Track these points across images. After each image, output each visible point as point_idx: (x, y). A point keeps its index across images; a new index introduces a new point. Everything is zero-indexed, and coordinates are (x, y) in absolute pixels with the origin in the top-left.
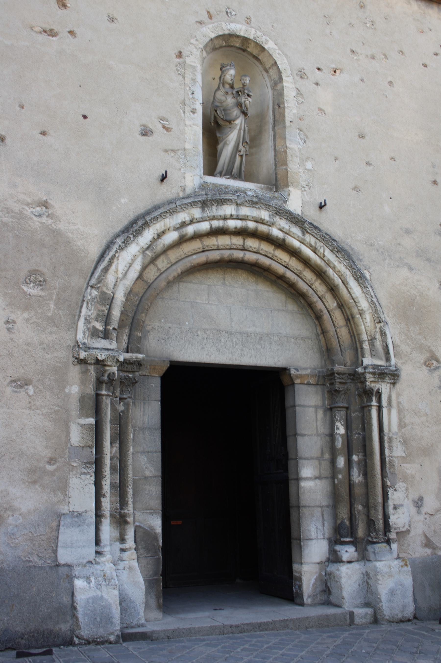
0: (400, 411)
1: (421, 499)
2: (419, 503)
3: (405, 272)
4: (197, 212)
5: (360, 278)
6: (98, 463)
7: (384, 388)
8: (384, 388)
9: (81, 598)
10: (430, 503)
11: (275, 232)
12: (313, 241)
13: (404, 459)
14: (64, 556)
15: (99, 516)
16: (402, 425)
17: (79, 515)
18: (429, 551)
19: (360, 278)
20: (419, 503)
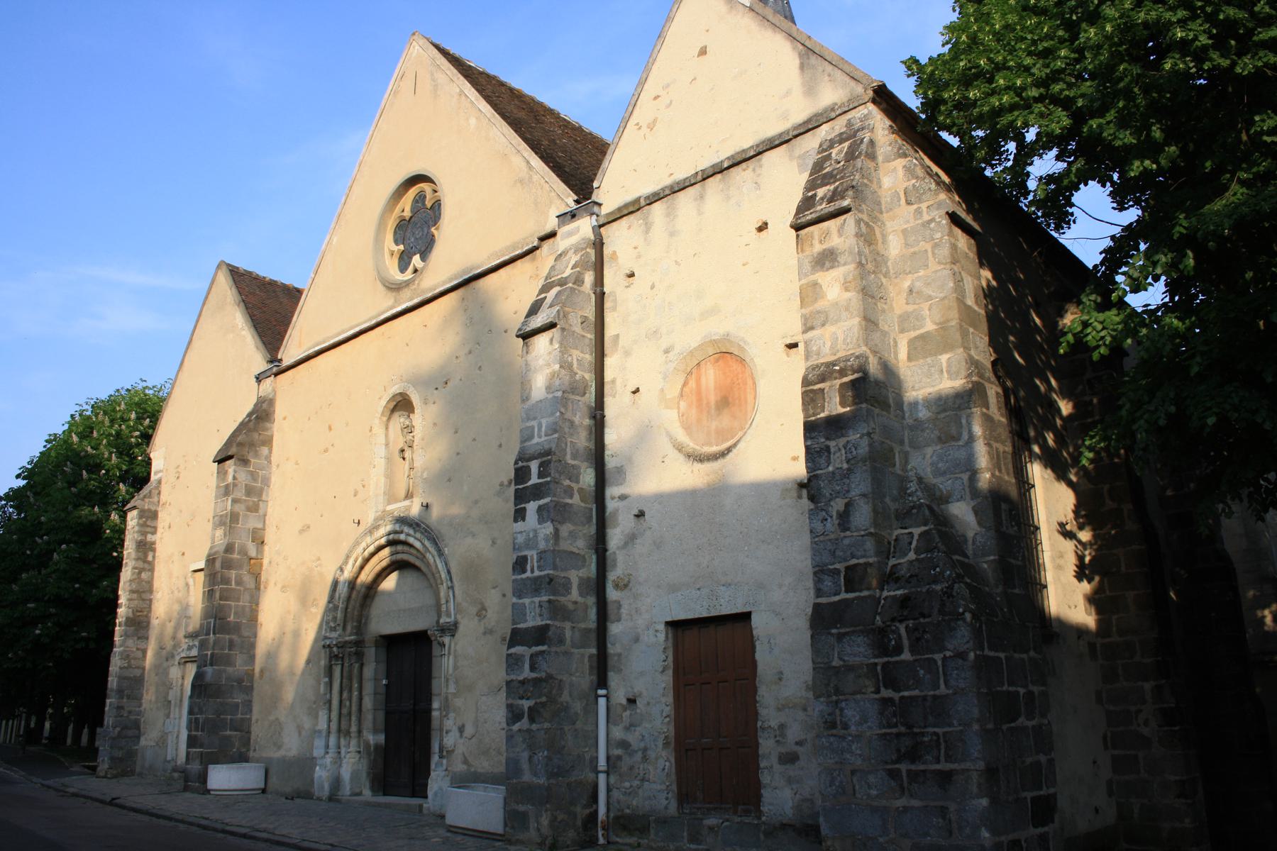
0: (455, 657)
1: (463, 726)
2: (461, 729)
3: (469, 540)
4: (368, 540)
5: (440, 553)
6: (330, 702)
7: (446, 640)
8: (446, 640)
9: (316, 775)
10: (469, 731)
11: (402, 537)
12: (418, 535)
13: (455, 695)
14: (315, 754)
15: (329, 732)
16: (456, 668)
17: (320, 731)
18: (465, 767)
19: (440, 553)
20: (461, 729)
